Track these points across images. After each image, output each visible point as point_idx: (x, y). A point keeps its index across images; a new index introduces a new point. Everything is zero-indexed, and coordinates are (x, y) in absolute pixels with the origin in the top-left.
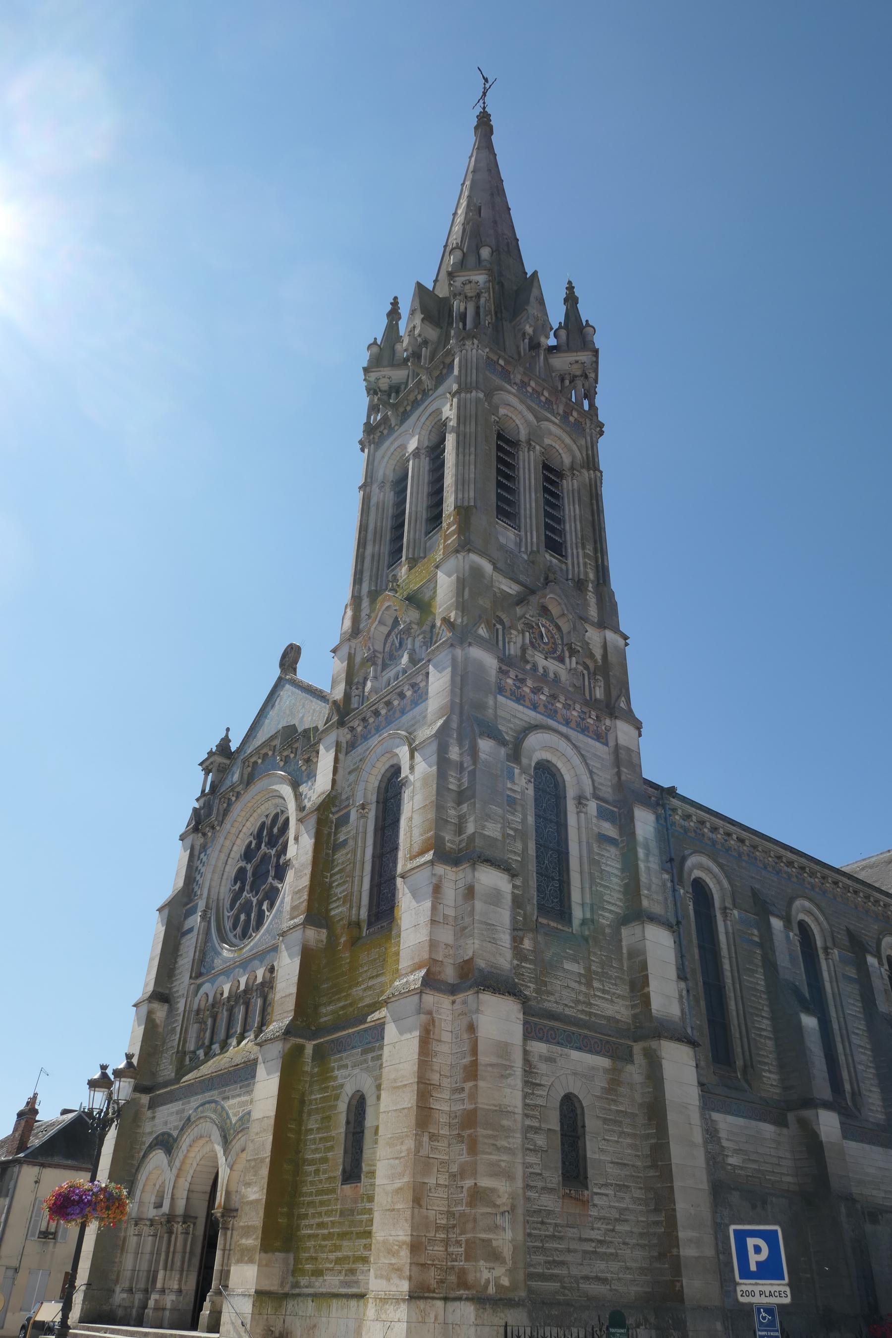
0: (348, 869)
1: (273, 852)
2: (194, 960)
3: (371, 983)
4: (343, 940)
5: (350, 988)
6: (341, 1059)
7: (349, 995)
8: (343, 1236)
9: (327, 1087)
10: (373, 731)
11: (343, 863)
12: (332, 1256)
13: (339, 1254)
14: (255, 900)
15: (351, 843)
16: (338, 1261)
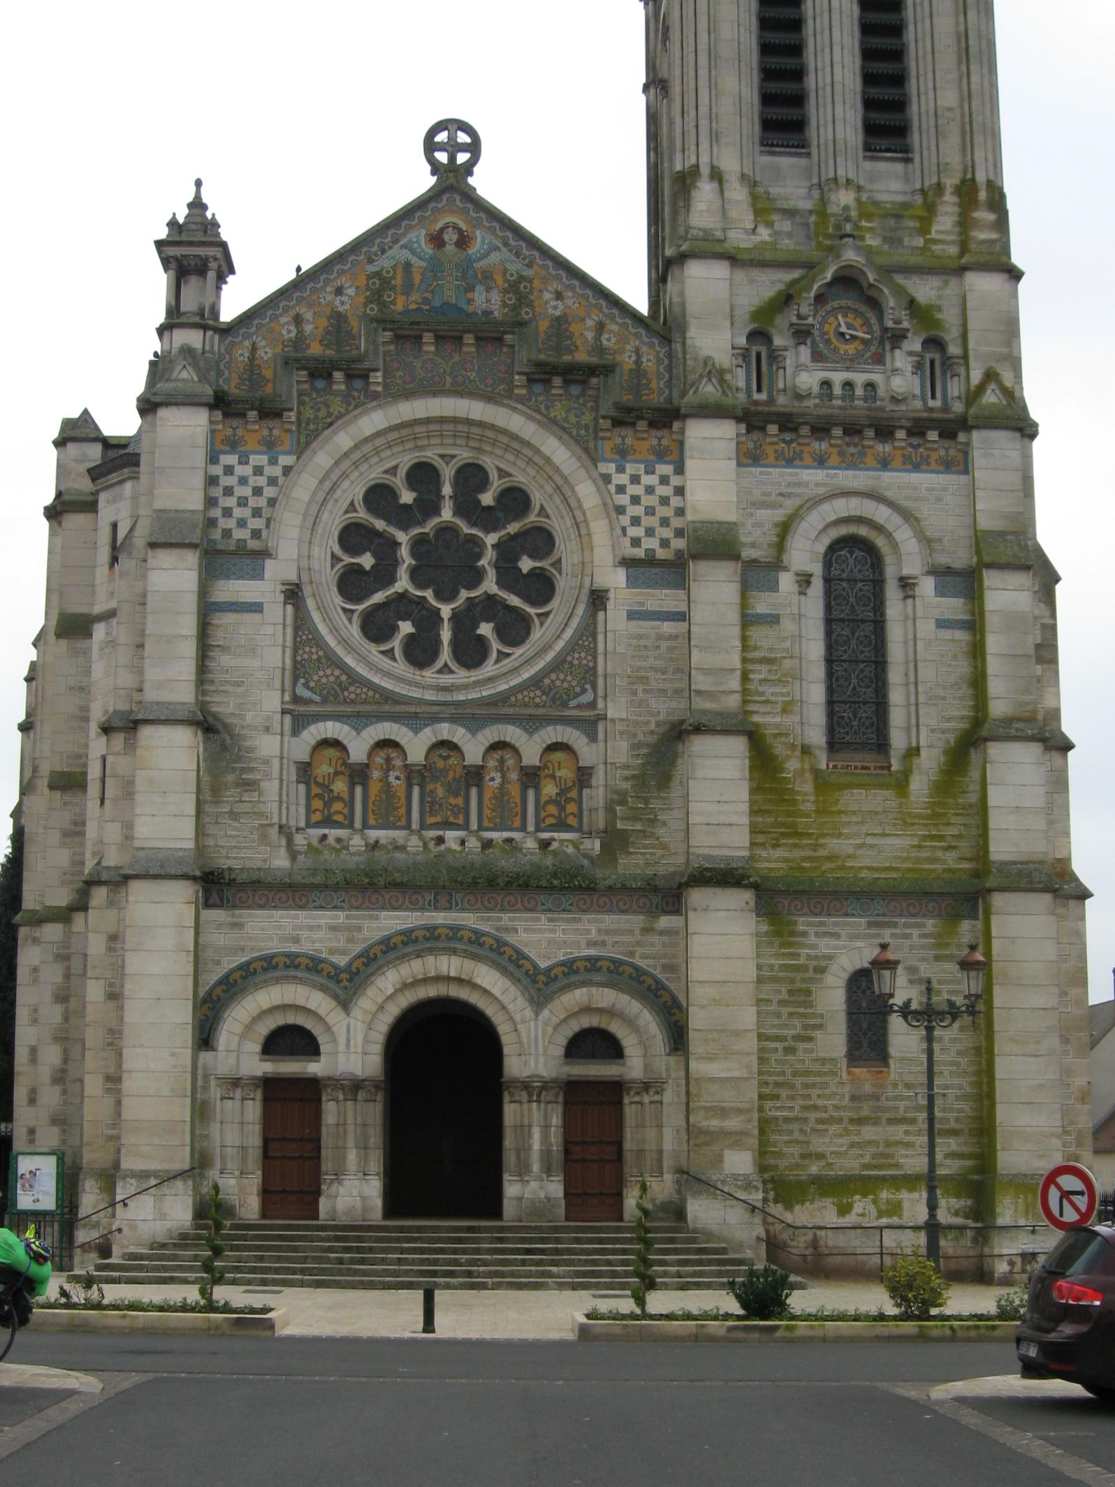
0: (787, 664)
1: (491, 539)
2: (284, 669)
3: (870, 840)
4: (793, 765)
5: (824, 835)
6: (821, 924)
7: (815, 847)
8: (860, 1121)
9: (799, 955)
10: (808, 460)
11: (771, 650)
12: (845, 1141)
13: (857, 1139)
14: (446, 611)
15: (788, 626)
16: (853, 1145)
